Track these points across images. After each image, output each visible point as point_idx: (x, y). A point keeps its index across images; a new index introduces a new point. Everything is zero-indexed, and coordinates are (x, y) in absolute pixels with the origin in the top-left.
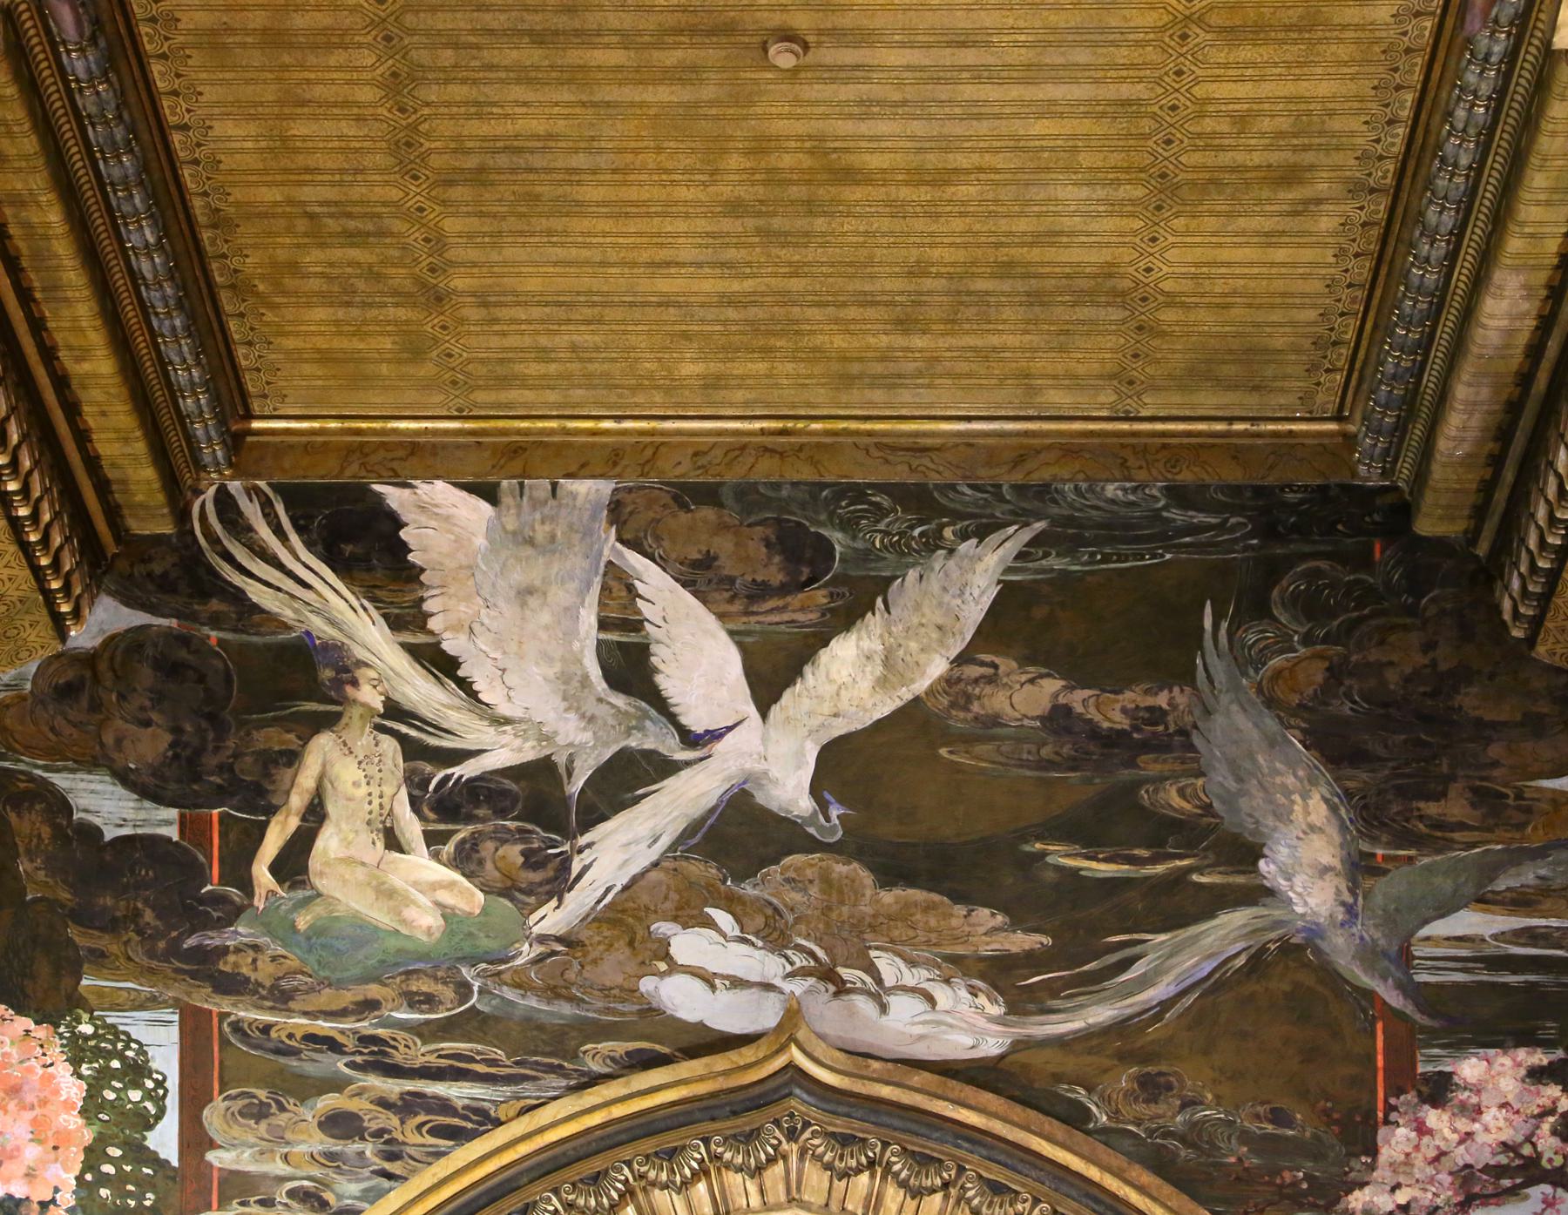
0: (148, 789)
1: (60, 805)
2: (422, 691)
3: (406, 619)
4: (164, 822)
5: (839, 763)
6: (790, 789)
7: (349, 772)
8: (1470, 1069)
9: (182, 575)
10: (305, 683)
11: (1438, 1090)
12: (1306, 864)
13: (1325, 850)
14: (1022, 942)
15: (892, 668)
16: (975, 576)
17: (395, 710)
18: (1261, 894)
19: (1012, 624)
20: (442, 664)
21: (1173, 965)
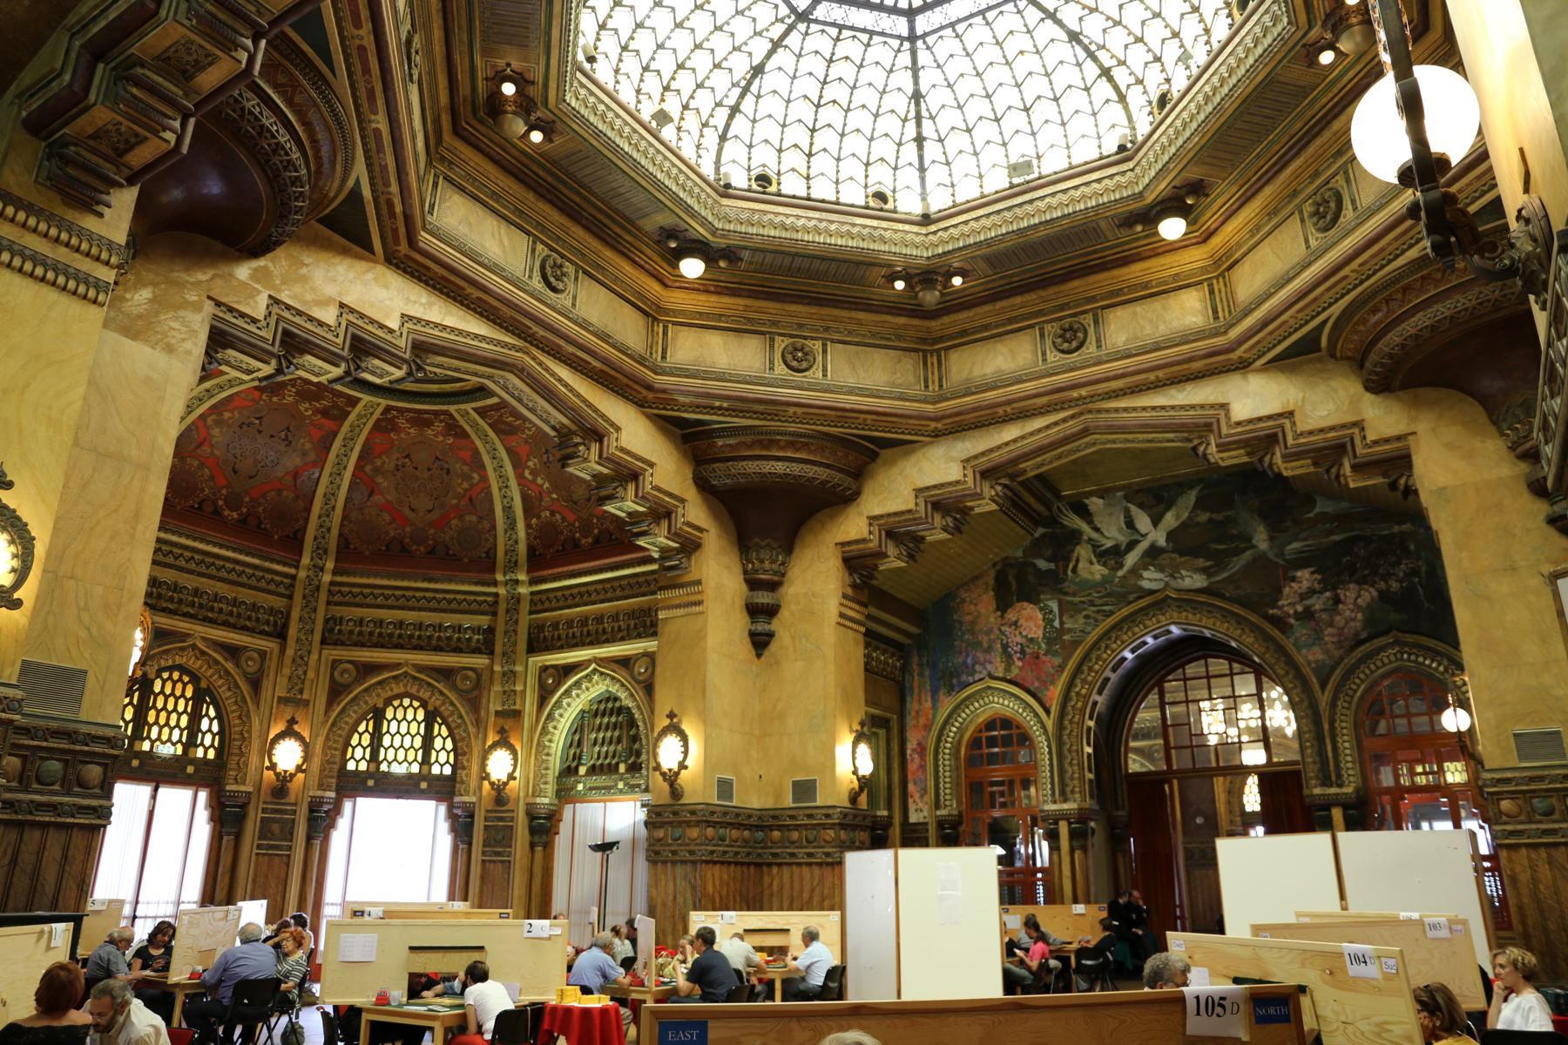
0: (1049, 560)
1: (1034, 565)
2: (1094, 535)
3: (1090, 522)
4: (1052, 566)
5: (1171, 536)
6: (1162, 542)
7: (1083, 552)
8: (1299, 574)
9: (1053, 521)
10: (1074, 537)
11: (1293, 579)
13: (1264, 536)
15: (1178, 516)
16: (1192, 496)
17: (1090, 539)
18: (1254, 547)
19: (1200, 504)
20: (1097, 530)
21: (1238, 563)
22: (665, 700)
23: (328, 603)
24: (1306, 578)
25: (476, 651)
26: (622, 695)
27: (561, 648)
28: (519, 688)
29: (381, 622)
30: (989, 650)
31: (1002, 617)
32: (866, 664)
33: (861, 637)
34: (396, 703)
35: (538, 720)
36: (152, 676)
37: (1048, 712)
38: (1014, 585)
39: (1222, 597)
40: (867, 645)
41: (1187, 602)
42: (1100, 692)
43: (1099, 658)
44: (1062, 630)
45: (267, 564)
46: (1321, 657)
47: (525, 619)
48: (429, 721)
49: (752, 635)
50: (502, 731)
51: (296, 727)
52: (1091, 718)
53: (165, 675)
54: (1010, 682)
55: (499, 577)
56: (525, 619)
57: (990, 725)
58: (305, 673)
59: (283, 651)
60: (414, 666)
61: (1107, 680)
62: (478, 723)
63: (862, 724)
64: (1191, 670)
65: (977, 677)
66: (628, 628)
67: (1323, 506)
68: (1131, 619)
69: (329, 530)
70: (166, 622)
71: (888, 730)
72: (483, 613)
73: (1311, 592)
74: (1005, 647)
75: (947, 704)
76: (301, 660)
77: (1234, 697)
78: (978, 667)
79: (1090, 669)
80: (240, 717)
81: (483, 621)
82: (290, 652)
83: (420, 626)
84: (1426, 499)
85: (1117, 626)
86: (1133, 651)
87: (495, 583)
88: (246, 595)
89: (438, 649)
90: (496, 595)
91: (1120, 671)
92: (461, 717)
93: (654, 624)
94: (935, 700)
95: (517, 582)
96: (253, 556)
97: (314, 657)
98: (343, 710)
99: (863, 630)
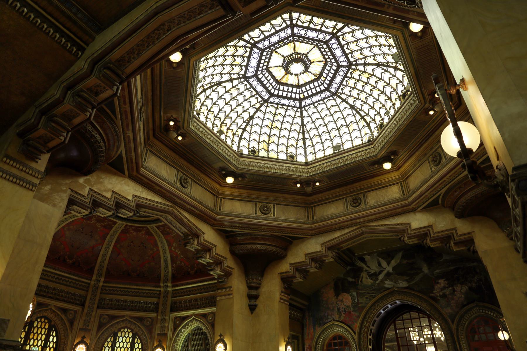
0: (353, 278)
2: (368, 269)
3: (366, 264)
4: (354, 280)
5: (394, 268)
6: (391, 271)
7: (364, 275)
8: (440, 281)
10: (361, 270)
11: (438, 283)
12: (425, 269)
14: (408, 278)
16: (400, 255)
17: (366, 270)
18: (423, 272)
19: (403, 257)
20: (368, 267)
21: (418, 278)
22: (218, 330)
23: (101, 293)
24: (442, 282)
25: (152, 311)
26: (203, 328)
27: (182, 310)
28: (166, 325)
30: (333, 310)
31: (337, 298)
32: (290, 316)
33: (288, 307)
34: (122, 330)
35: (173, 337)
36: (34, 320)
37: (355, 333)
38: (341, 287)
39: (413, 290)
40: (290, 309)
41: (401, 292)
42: (373, 325)
43: (372, 313)
44: (358, 303)
45: (80, 279)
46: (451, 311)
47: (170, 300)
48: (133, 338)
49: (250, 306)
50: (160, 341)
51: (85, 340)
52: (370, 335)
53: (39, 320)
54: (341, 322)
55: (162, 285)
56: (170, 300)
57: (334, 338)
58: (90, 319)
59: (83, 310)
60: (130, 316)
61: (375, 321)
62: (151, 338)
63: (289, 338)
64: (405, 316)
65: (329, 320)
66: (206, 303)
67: (445, 257)
68: (382, 299)
69: (103, 267)
70: (42, 300)
71: (298, 340)
72: (155, 297)
73: (445, 288)
74: (338, 309)
75: (319, 330)
77: (421, 326)
78: (329, 317)
79: (369, 317)
80: (64, 336)
81: (155, 300)
83: (132, 302)
84: (480, 254)
85: (377, 301)
86: (384, 310)
87: (160, 287)
88: (72, 290)
89: (139, 310)
90: (160, 291)
91: (380, 317)
92: (145, 336)
93: (215, 302)
94: (314, 329)
95: (168, 286)
96: (76, 276)
97: (94, 313)
98: (102, 333)
99: (288, 304)
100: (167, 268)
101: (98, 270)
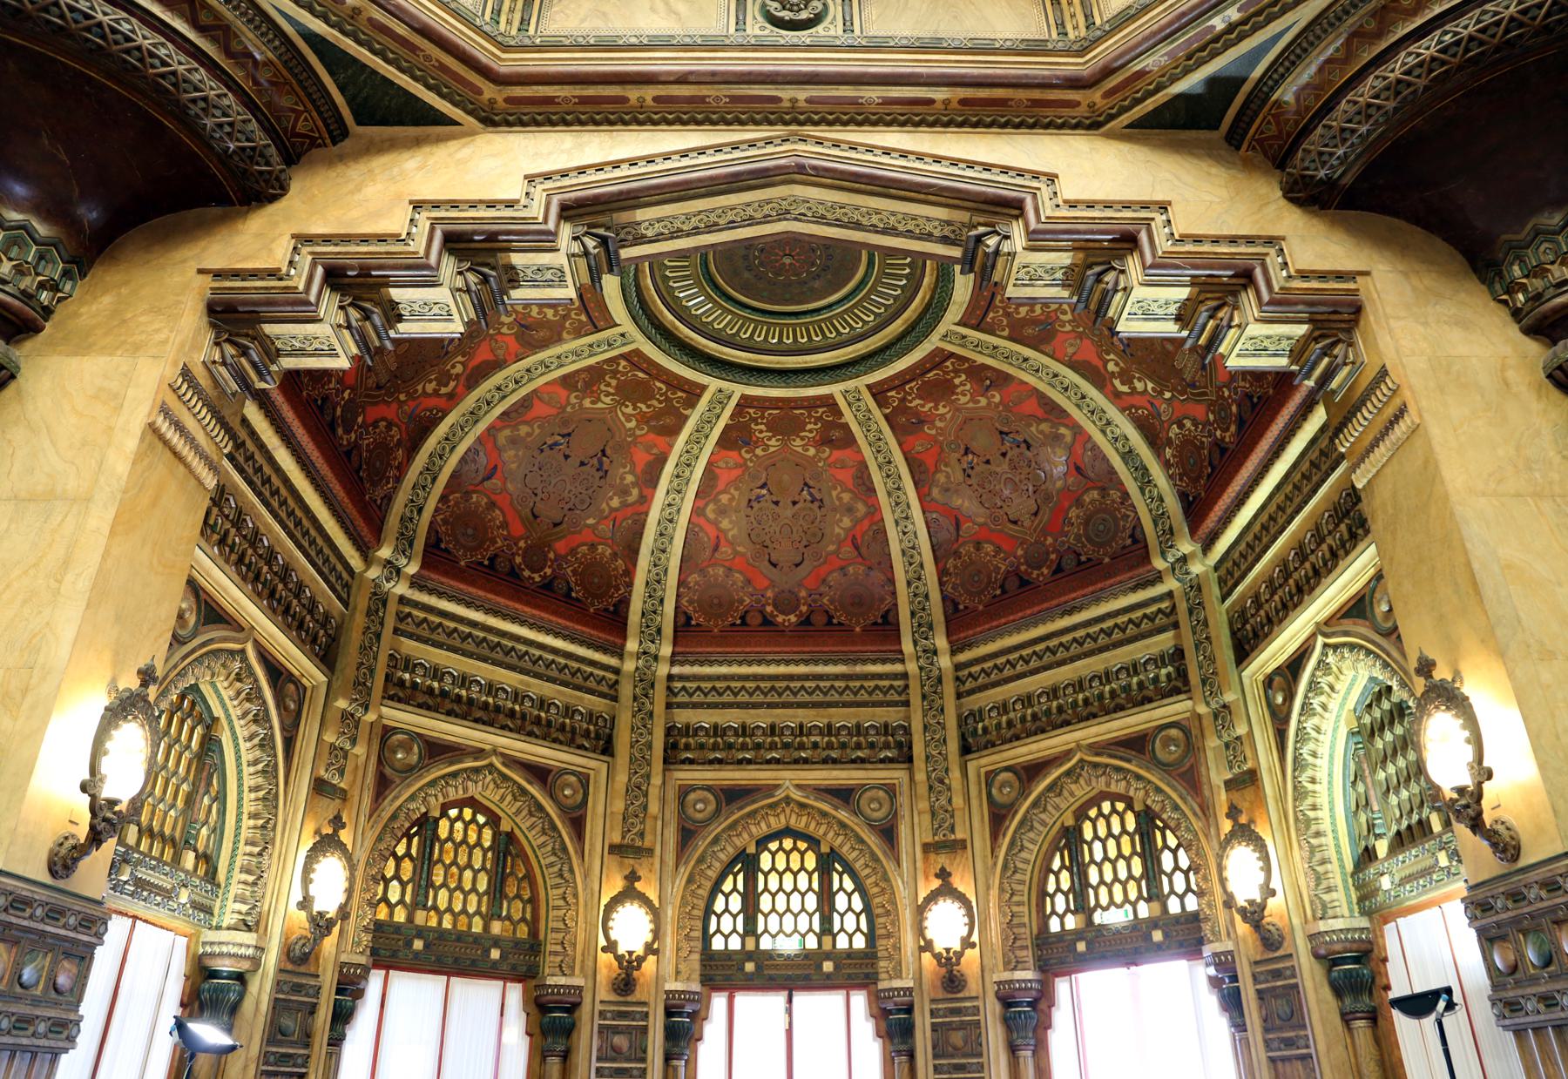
29: (1029, 697)
45: (859, 669)
55: (1159, 564)
69: (927, 597)
72: (1160, 630)
76: (938, 784)
81: (1163, 642)
82: (920, 776)
87: (1158, 578)
95: (1184, 559)
96: (835, 663)
98: (1012, 843)
100: (1154, 489)
101: (913, 614)
